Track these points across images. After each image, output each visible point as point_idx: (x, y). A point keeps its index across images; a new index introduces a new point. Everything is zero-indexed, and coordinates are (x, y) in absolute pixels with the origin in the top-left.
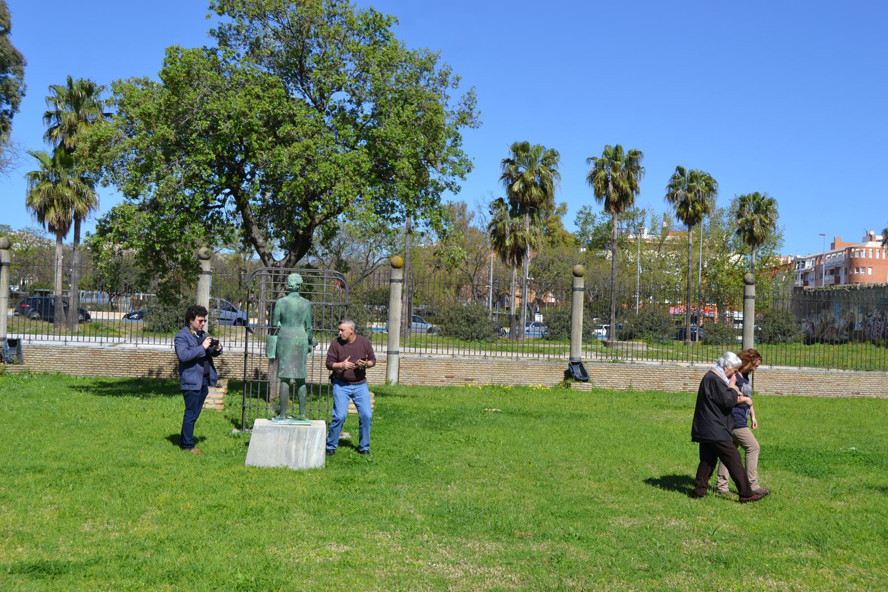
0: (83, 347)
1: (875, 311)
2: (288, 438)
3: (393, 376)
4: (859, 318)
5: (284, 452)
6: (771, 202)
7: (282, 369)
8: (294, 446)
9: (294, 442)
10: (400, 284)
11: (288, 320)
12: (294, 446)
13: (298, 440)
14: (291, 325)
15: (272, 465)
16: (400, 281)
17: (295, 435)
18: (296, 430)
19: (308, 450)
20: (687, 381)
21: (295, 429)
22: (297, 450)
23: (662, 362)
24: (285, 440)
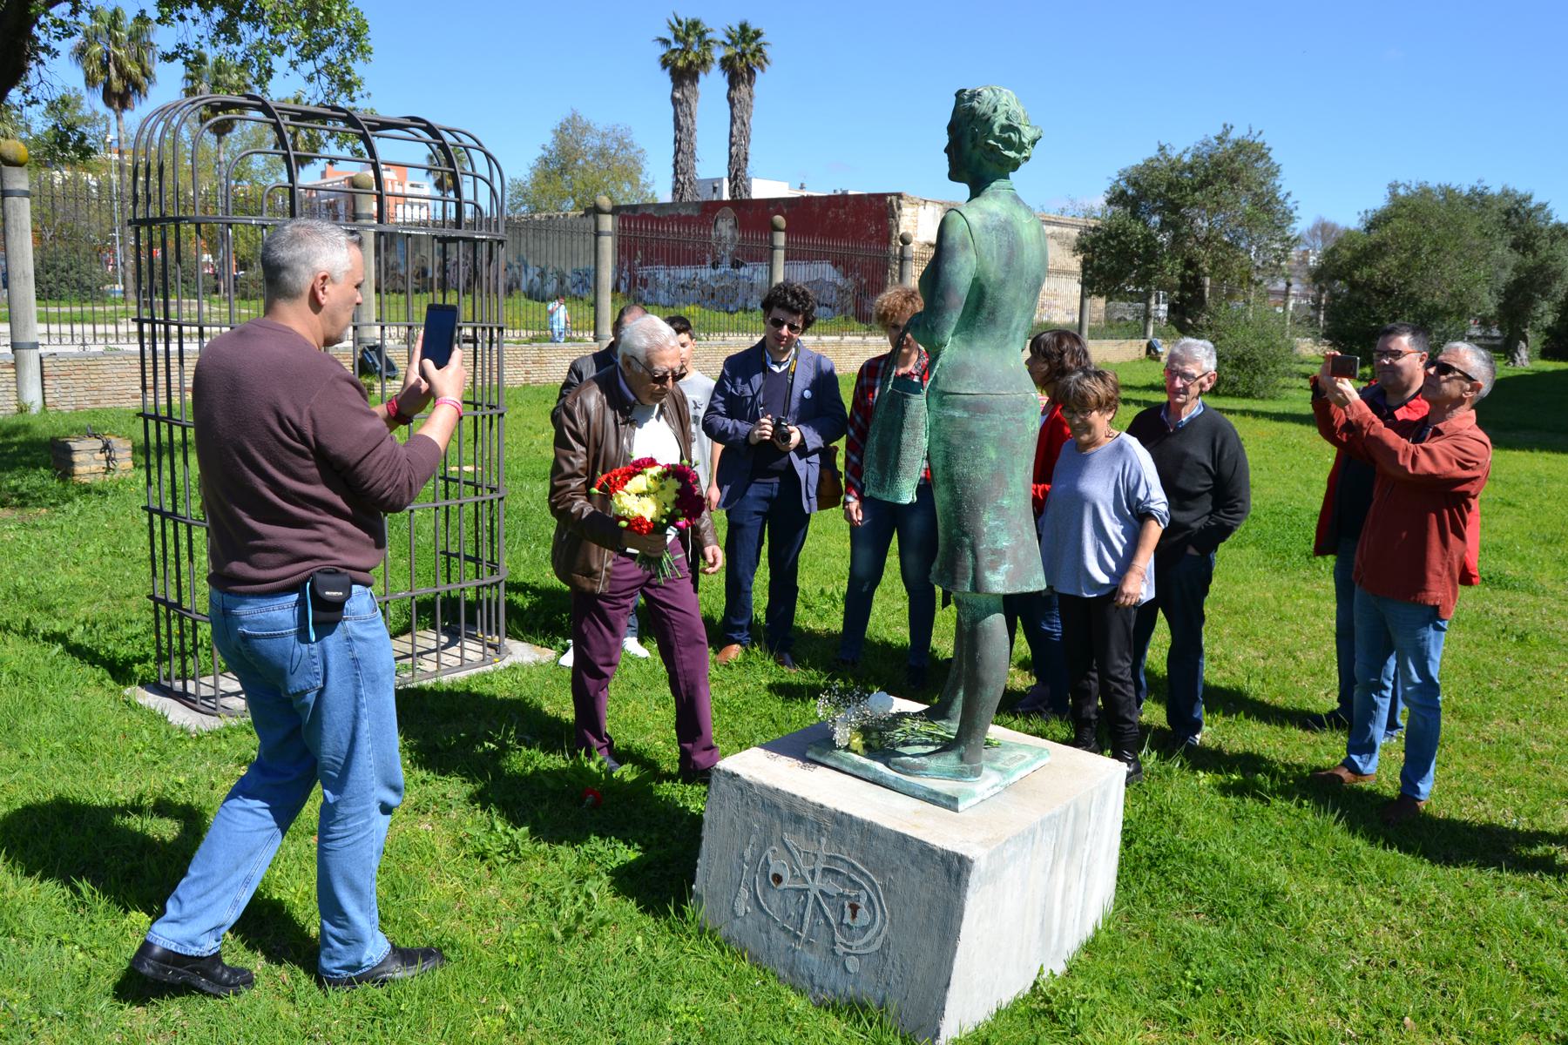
3: (33, 395)
5: (1038, 921)
7: (999, 554)
10: (27, 201)
11: (1002, 314)
16: (26, 194)
19: (1088, 875)
20: (530, 366)
22: (1067, 889)
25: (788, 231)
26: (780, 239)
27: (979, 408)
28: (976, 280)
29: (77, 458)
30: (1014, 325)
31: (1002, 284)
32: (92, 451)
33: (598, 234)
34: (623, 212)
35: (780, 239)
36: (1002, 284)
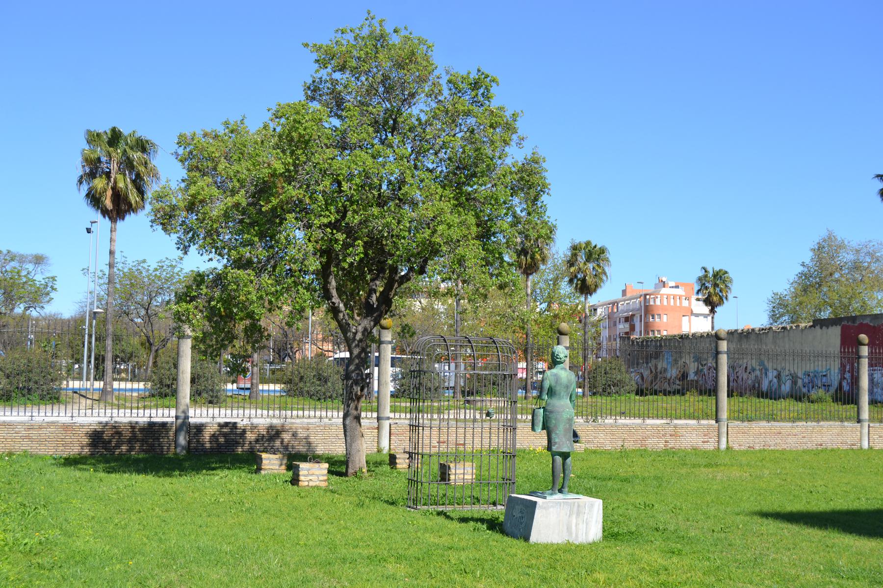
0: (53, 423)
1: (710, 360)
2: (568, 513)
4: (692, 367)
5: (565, 528)
6: (602, 251)
7: (556, 443)
8: (574, 521)
9: (574, 516)
11: (557, 393)
12: (574, 521)
13: (578, 514)
14: (560, 398)
15: (555, 541)
16: (390, 343)
17: (575, 509)
18: (576, 504)
19: (587, 524)
20: (668, 438)
21: (574, 503)
22: (577, 525)
23: (616, 419)
24: (566, 514)
25: (871, 344)
26: (865, 351)
27: (551, 412)
28: (550, 386)
29: (397, 461)
30: (562, 395)
31: (555, 386)
32: (404, 459)
33: (717, 353)
34: (845, 323)
35: (865, 351)
36: (555, 386)
